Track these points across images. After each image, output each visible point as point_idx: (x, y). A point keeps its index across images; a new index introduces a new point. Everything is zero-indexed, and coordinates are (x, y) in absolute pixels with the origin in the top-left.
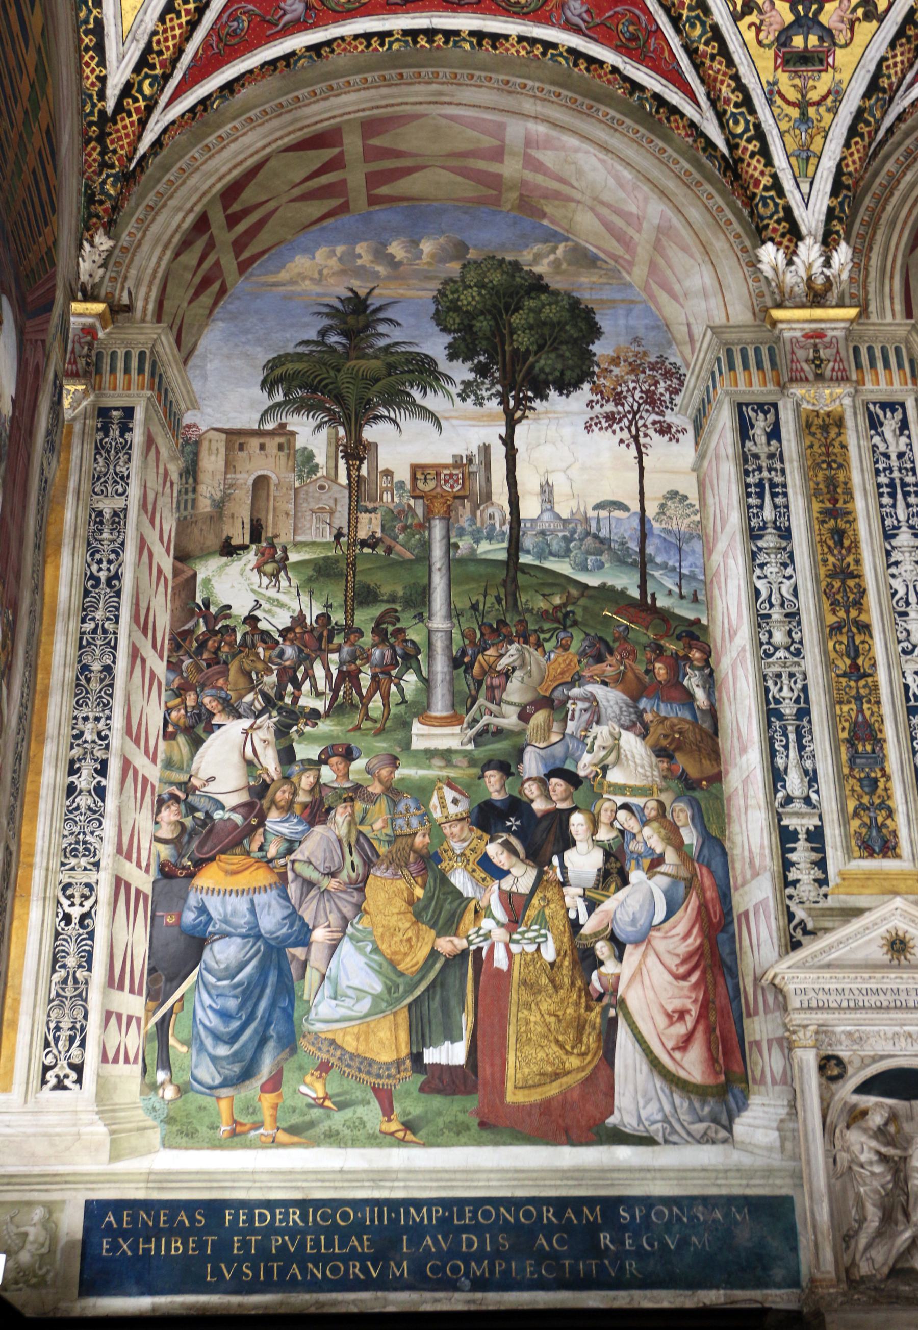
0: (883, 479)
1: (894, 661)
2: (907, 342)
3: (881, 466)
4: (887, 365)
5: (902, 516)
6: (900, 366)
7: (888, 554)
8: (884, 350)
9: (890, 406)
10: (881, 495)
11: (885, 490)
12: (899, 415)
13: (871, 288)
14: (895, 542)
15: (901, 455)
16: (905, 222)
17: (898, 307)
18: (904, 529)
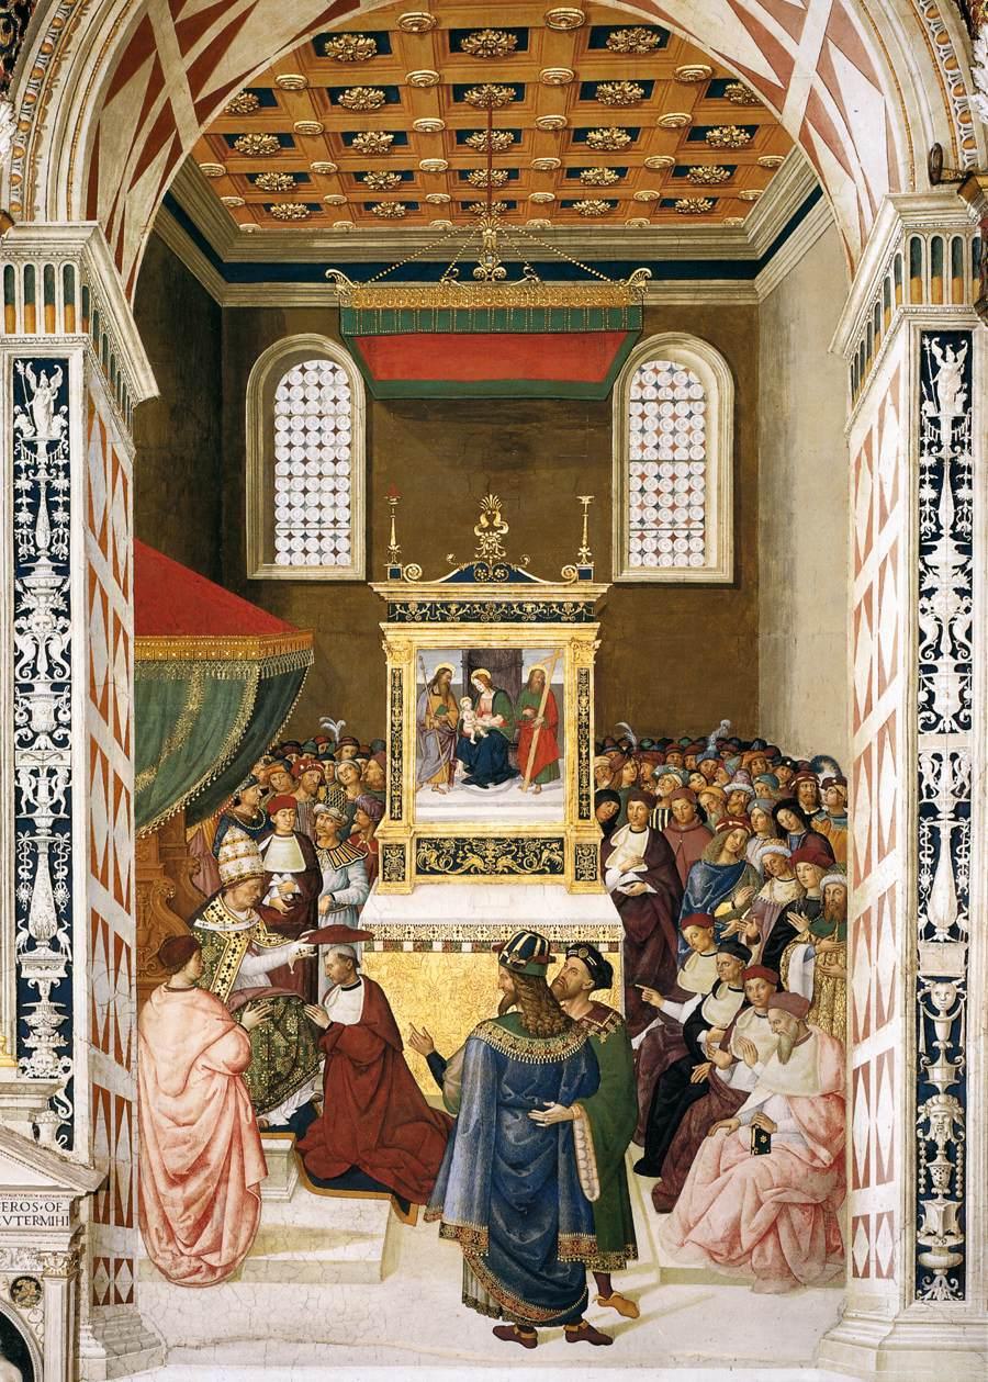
0: (24, 484)
1: (8, 755)
2: (83, 258)
3: (22, 463)
4: (49, 299)
5: (42, 538)
6: (69, 300)
7: (18, 597)
8: (48, 270)
9: (45, 366)
10: (18, 508)
11: (25, 500)
12: (57, 380)
13: (42, 168)
14: (28, 581)
15: (52, 446)
16: (106, 47)
17: (78, 198)
18: (43, 560)
